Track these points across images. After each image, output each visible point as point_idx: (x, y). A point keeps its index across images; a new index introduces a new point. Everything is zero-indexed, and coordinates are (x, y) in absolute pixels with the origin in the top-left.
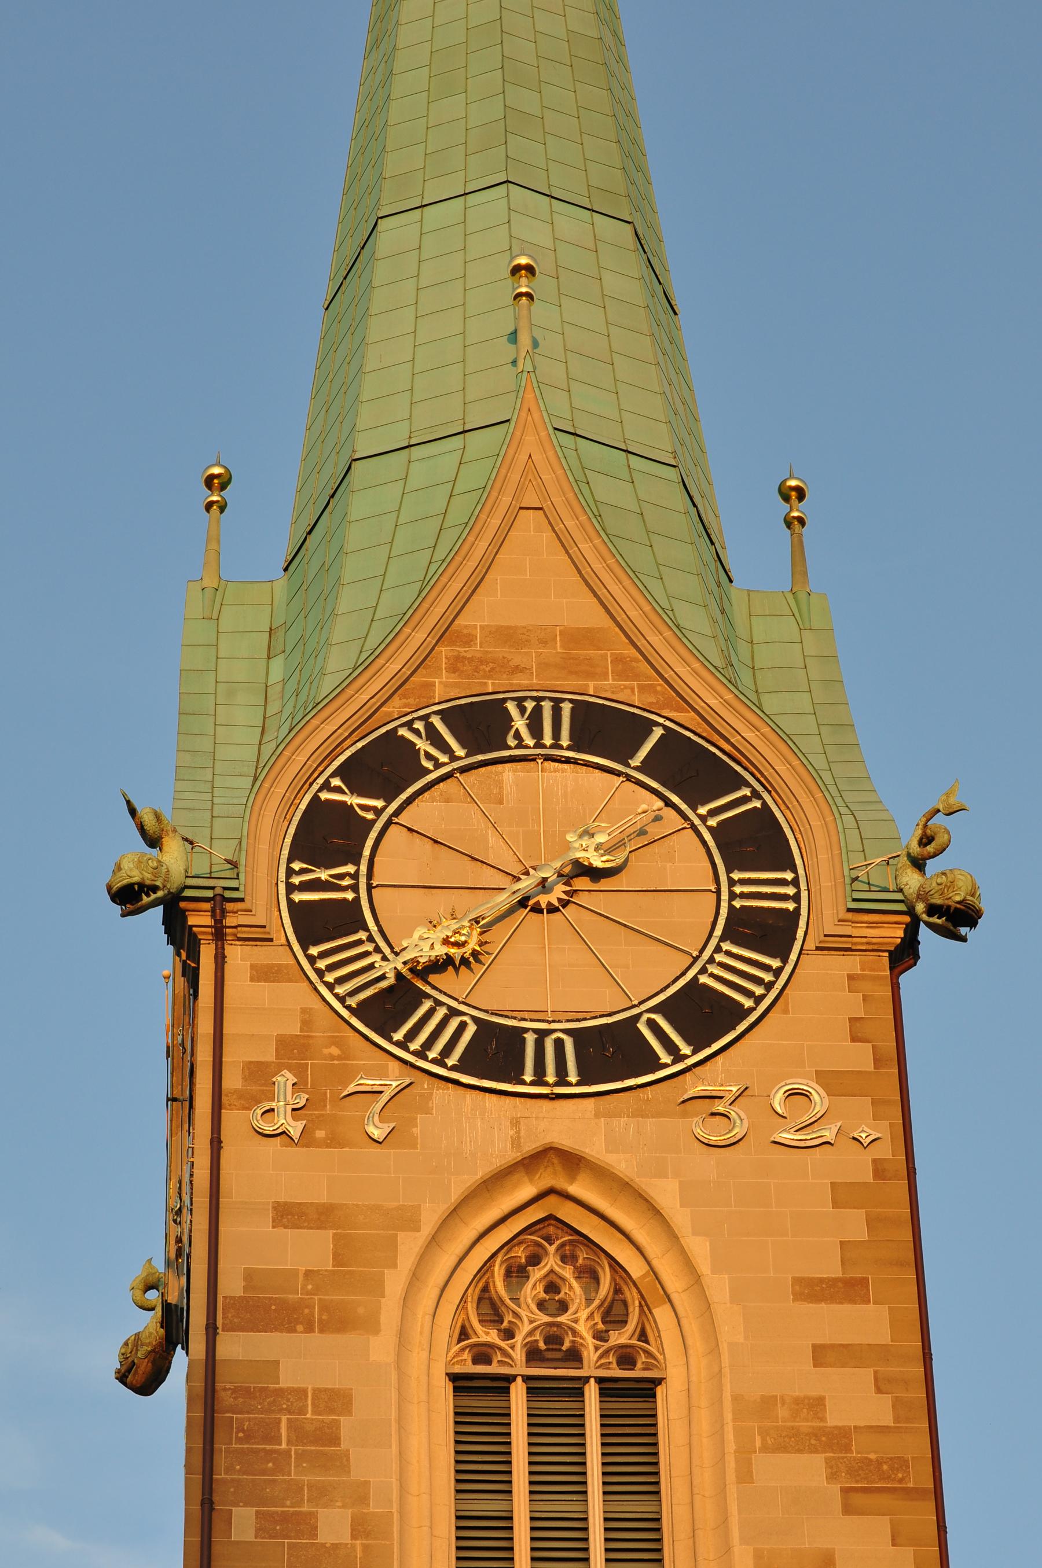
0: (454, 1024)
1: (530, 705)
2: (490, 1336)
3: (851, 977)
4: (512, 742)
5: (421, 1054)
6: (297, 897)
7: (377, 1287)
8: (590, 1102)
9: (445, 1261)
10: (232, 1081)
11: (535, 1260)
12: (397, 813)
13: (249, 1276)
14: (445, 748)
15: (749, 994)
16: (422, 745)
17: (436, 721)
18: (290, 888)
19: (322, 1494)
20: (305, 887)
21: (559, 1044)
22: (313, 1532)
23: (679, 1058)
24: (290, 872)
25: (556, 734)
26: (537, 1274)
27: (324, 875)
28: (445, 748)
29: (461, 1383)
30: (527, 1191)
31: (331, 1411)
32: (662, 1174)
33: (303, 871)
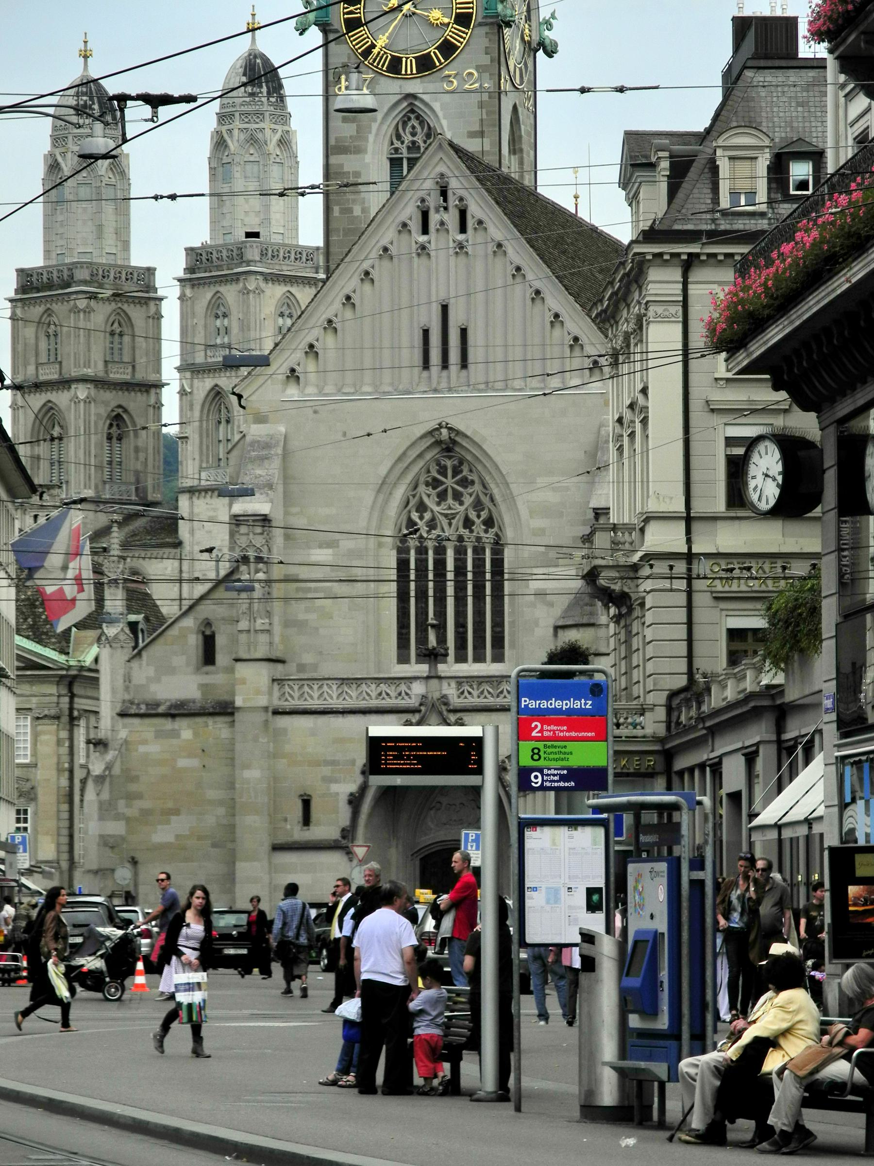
2: (397, 144)
3: (487, 33)
6: (346, 16)
7: (367, 141)
8: (419, 80)
9: (385, 127)
10: (331, 78)
11: (409, 119)
13: (336, 139)
15: (459, 41)
18: (344, 14)
19: (354, 201)
20: (348, 13)
21: (411, 61)
22: (352, 212)
23: (441, 64)
24: (344, 8)
26: (410, 125)
27: (352, 8)
29: (391, 160)
30: (405, 104)
31: (356, 177)
32: (436, 101)
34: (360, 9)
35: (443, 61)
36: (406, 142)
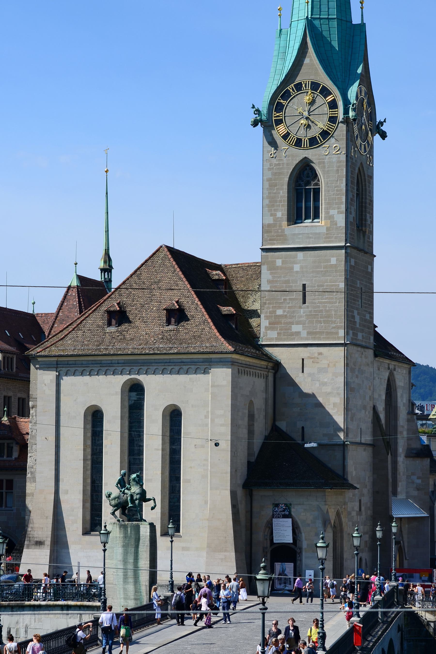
0: (294, 138)
1: (305, 82)
4: (302, 89)
5: (289, 143)
6: (275, 118)
11: (306, 169)
12: (288, 103)
14: (294, 91)
15: (330, 131)
16: (291, 90)
17: (293, 86)
24: (274, 114)
25: (308, 88)
26: (306, 172)
28: (294, 91)
33: (276, 114)
34: (282, 114)
35: (322, 140)
36: (304, 181)
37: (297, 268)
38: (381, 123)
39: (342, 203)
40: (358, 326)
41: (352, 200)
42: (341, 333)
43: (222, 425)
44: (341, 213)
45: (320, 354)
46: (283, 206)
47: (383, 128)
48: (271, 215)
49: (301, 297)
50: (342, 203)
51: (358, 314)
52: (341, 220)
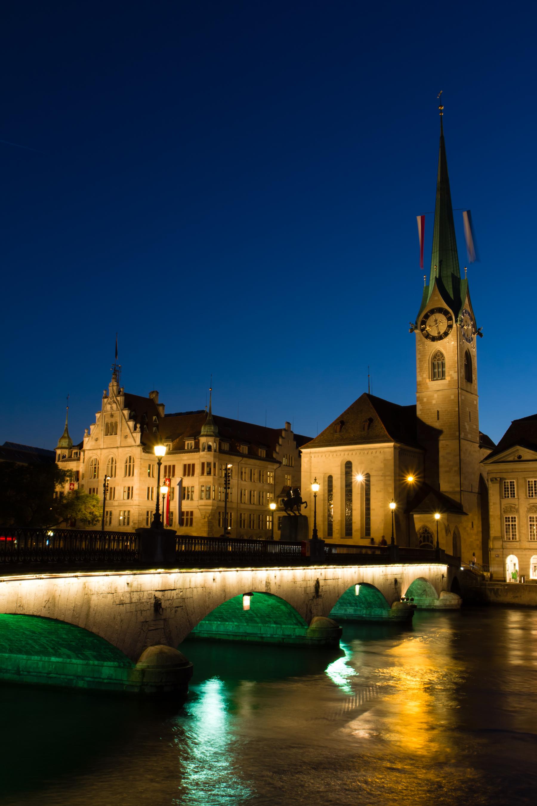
37: (434, 402)
38: (479, 329)
39: (456, 367)
40: (468, 430)
41: (461, 366)
42: (457, 434)
43: (390, 480)
44: (456, 372)
45: (447, 445)
46: (426, 371)
47: (480, 331)
48: (421, 376)
49: (437, 416)
50: (456, 367)
51: (468, 424)
52: (455, 376)
